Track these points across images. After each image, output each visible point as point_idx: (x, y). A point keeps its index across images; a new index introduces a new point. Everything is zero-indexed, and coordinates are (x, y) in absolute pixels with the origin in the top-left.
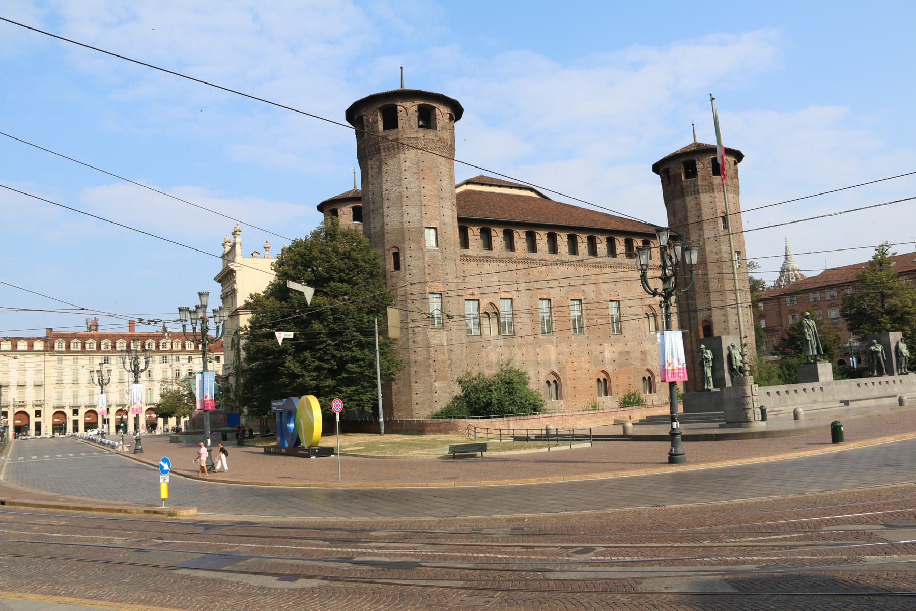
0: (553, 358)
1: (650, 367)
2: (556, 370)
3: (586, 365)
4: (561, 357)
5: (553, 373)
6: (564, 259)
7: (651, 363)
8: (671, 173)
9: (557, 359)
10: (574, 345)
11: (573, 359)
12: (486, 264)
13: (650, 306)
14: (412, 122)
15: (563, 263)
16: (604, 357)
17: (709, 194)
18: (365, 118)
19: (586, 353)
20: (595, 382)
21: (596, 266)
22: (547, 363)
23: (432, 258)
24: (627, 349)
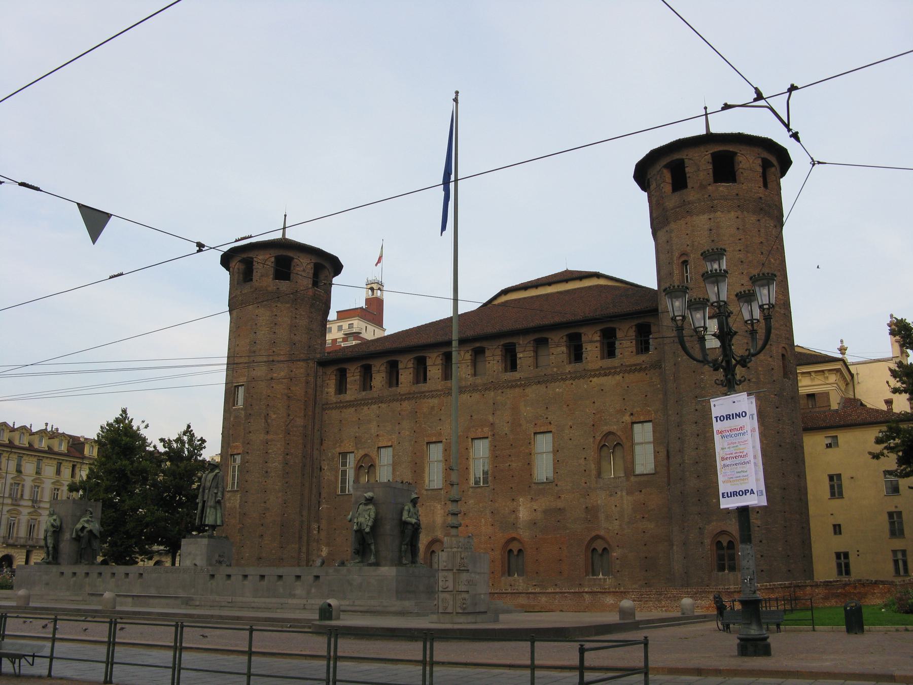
1: (602, 533)
12: (366, 408)
13: (610, 433)
16: (517, 518)
17: (665, 230)
21: (512, 385)
23: (236, 417)
24: (560, 504)
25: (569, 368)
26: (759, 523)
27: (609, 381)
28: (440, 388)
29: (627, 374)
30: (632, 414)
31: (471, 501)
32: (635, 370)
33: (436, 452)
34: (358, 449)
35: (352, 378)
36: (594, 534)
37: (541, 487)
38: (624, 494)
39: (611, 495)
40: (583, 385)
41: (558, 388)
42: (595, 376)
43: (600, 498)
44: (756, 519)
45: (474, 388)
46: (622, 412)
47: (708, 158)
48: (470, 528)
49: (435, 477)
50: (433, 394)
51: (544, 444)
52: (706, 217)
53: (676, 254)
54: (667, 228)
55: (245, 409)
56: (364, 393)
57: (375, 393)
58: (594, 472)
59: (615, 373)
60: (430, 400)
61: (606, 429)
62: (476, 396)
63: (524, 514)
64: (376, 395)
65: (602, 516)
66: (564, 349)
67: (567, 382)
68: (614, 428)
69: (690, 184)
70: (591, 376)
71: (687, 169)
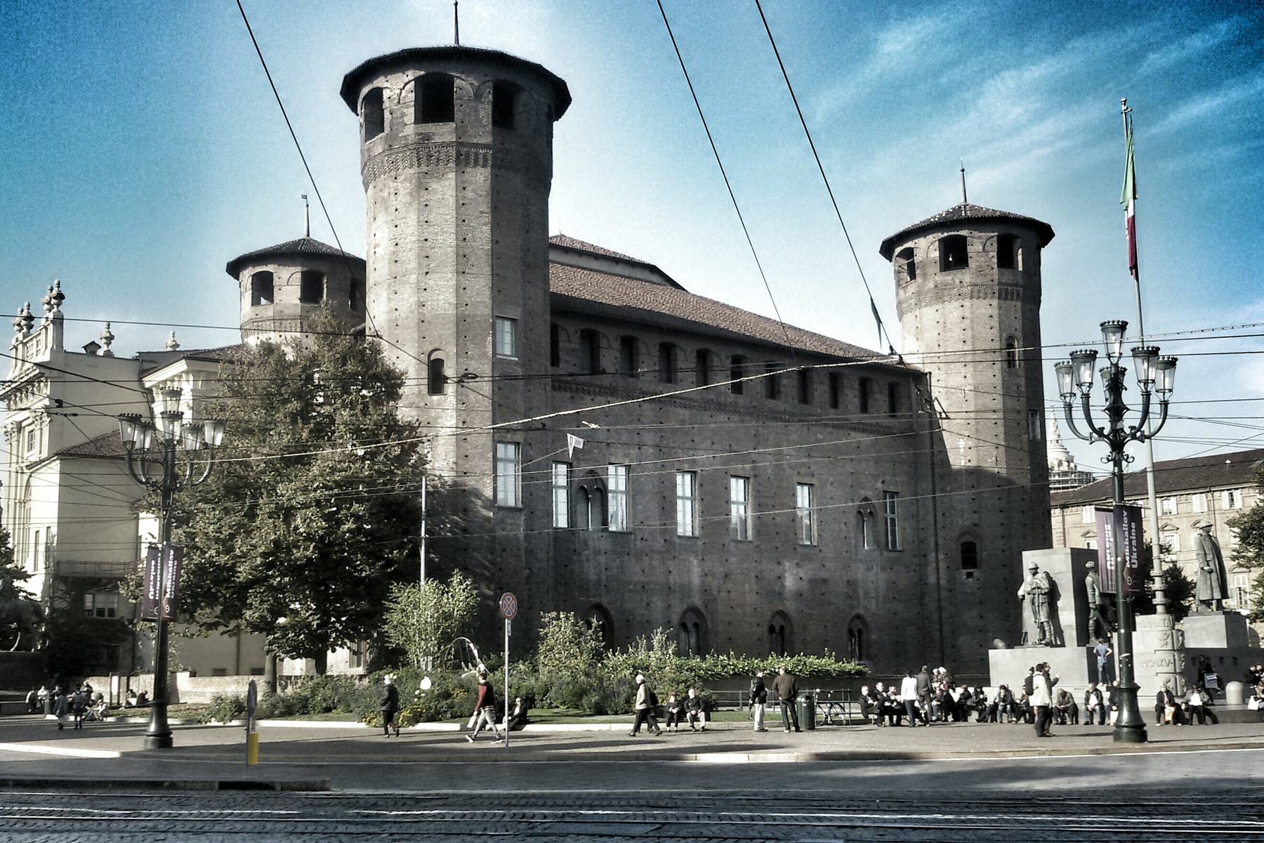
0: (696, 580)
1: (861, 612)
2: (697, 601)
4: (709, 579)
5: (694, 610)
7: (863, 602)
8: (917, 259)
9: (703, 583)
14: (482, 114)
16: (783, 586)
17: (987, 302)
18: (386, 94)
19: (753, 575)
20: (765, 629)
21: (776, 416)
24: (824, 575)
25: (832, 414)
27: (866, 439)
33: (684, 484)
35: (567, 345)
36: (854, 613)
37: (807, 550)
42: (854, 429)
43: (859, 572)
49: (686, 520)
51: (803, 496)
68: (869, 494)
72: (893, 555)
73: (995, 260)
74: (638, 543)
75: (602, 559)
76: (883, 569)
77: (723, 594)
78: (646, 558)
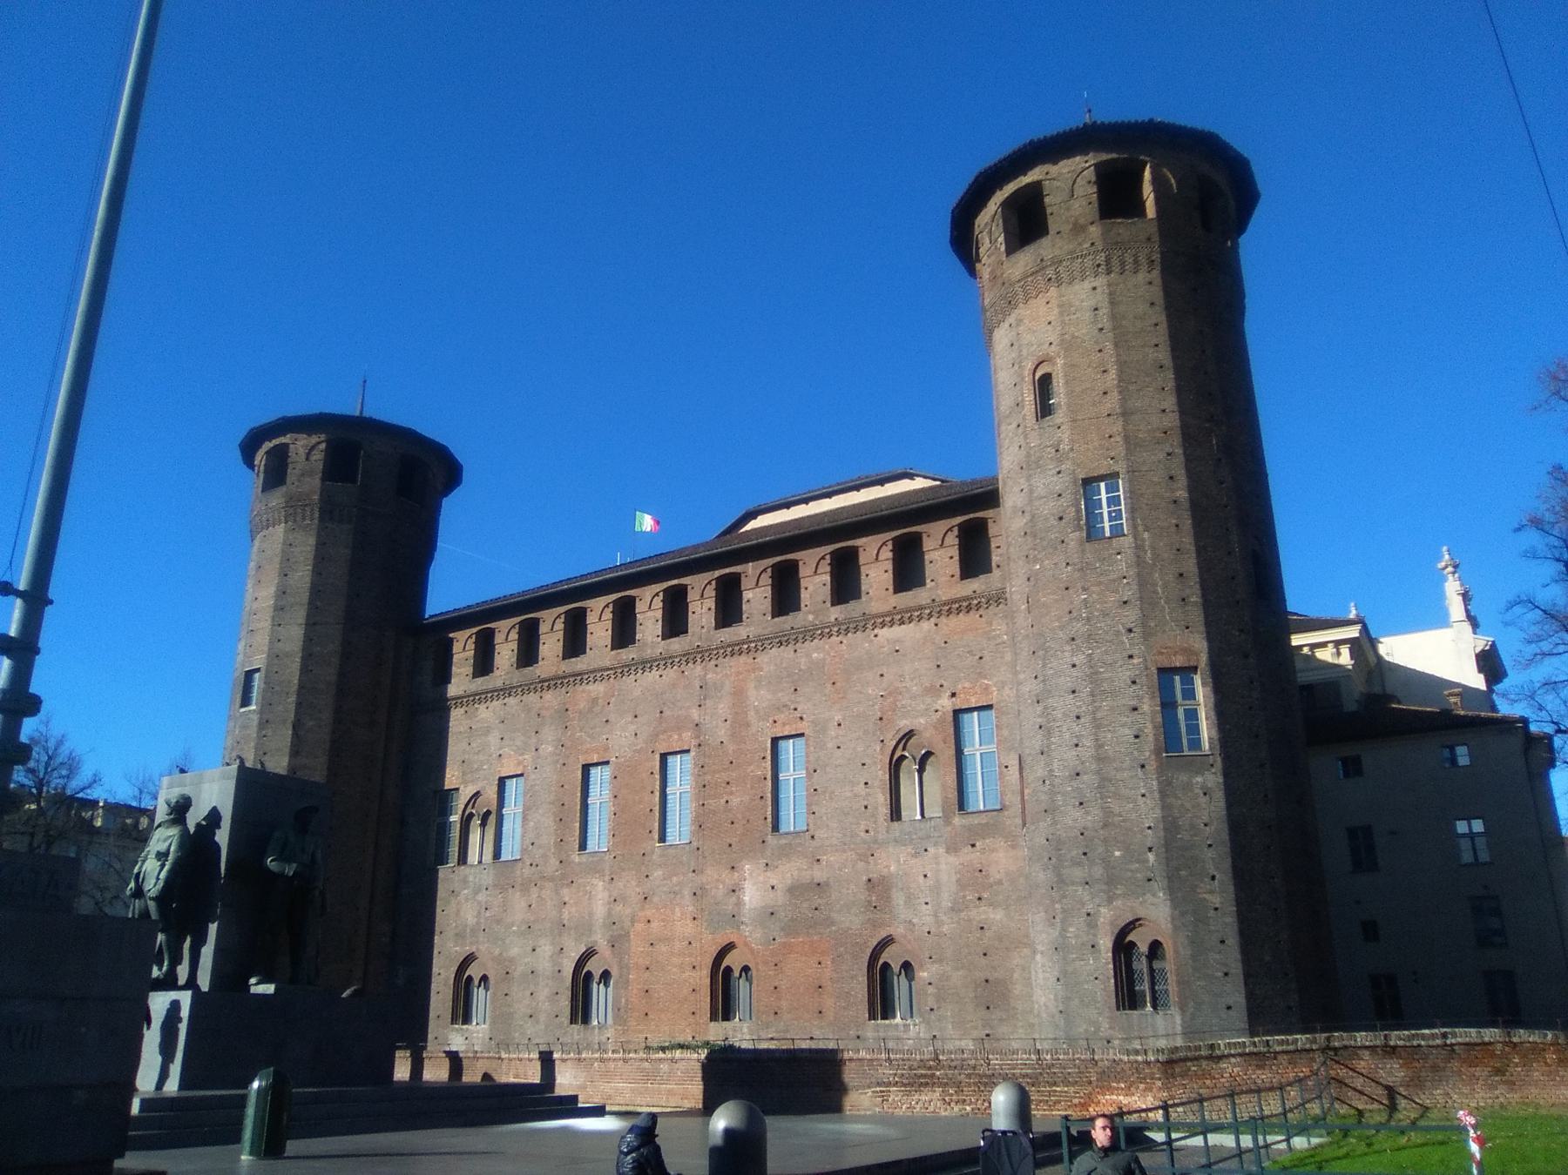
0: (600, 910)
1: (898, 930)
2: (601, 941)
3: (684, 928)
4: (618, 908)
6: (649, 653)
7: (903, 913)
9: (609, 914)
10: (658, 873)
11: (649, 913)
12: (482, 707)
15: (645, 664)
16: (739, 903)
17: (1006, 325)
19: (687, 893)
21: (735, 649)
22: (584, 927)
24: (819, 874)
25: (836, 613)
26: (1216, 900)
28: (608, 664)
29: (943, 619)
30: (953, 695)
31: (658, 873)
32: (959, 611)
34: (465, 783)
36: (883, 934)
38: (942, 850)
39: (916, 855)
40: (859, 644)
41: (815, 651)
42: (883, 625)
43: (893, 861)
44: (1211, 892)
45: (666, 661)
46: (935, 690)
47: (1090, 174)
48: (654, 925)
50: (597, 674)
52: (1087, 285)
53: (1030, 366)
54: (1011, 319)
55: (261, 712)
56: (480, 680)
57: (498, 678)
58: (884, 811)
59: (920, 618)
60: (591, 687)
61: (905, 724)
62: (671, 674)
63: (752, 896)
64: (499, 684)
65: (898, 898)
66: (827, 578)
67: (834, 638)
68: (919, 722)
69: (1053, 225)
70: (874, 626)
71: (1047, 200)
72: (983, 819)
73: (1003, 248)
74: (527, 871)
75: (481, 897)
76: (952, 849)
77: (639, 926)
78: (534, 890)
